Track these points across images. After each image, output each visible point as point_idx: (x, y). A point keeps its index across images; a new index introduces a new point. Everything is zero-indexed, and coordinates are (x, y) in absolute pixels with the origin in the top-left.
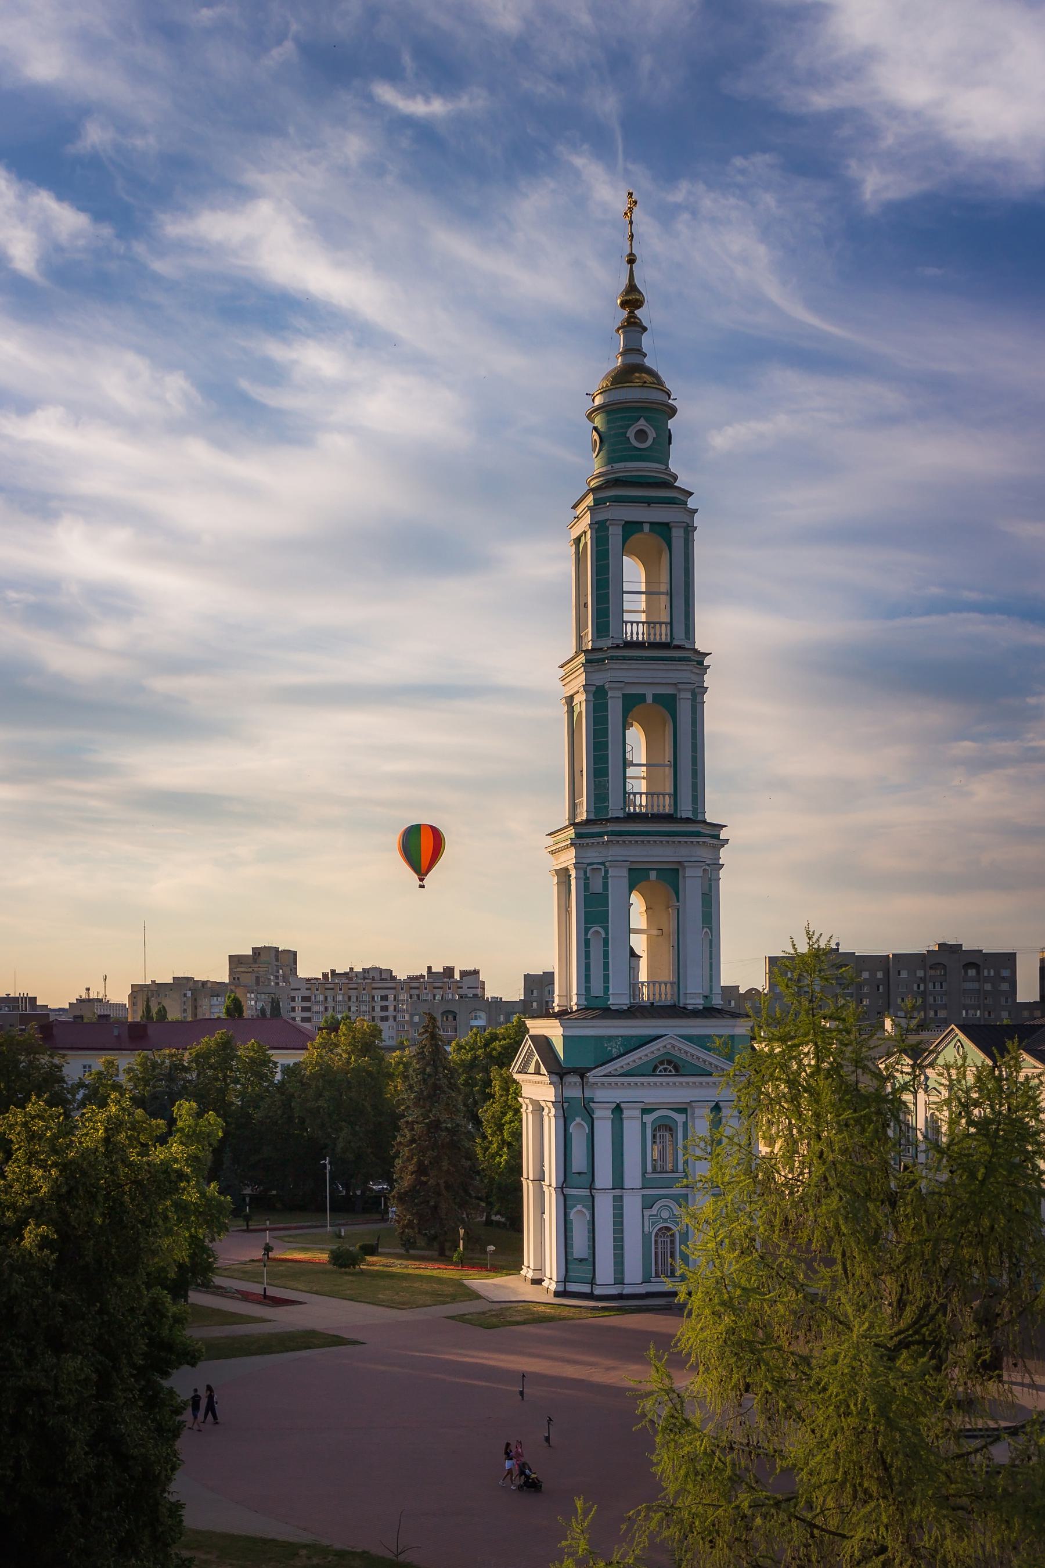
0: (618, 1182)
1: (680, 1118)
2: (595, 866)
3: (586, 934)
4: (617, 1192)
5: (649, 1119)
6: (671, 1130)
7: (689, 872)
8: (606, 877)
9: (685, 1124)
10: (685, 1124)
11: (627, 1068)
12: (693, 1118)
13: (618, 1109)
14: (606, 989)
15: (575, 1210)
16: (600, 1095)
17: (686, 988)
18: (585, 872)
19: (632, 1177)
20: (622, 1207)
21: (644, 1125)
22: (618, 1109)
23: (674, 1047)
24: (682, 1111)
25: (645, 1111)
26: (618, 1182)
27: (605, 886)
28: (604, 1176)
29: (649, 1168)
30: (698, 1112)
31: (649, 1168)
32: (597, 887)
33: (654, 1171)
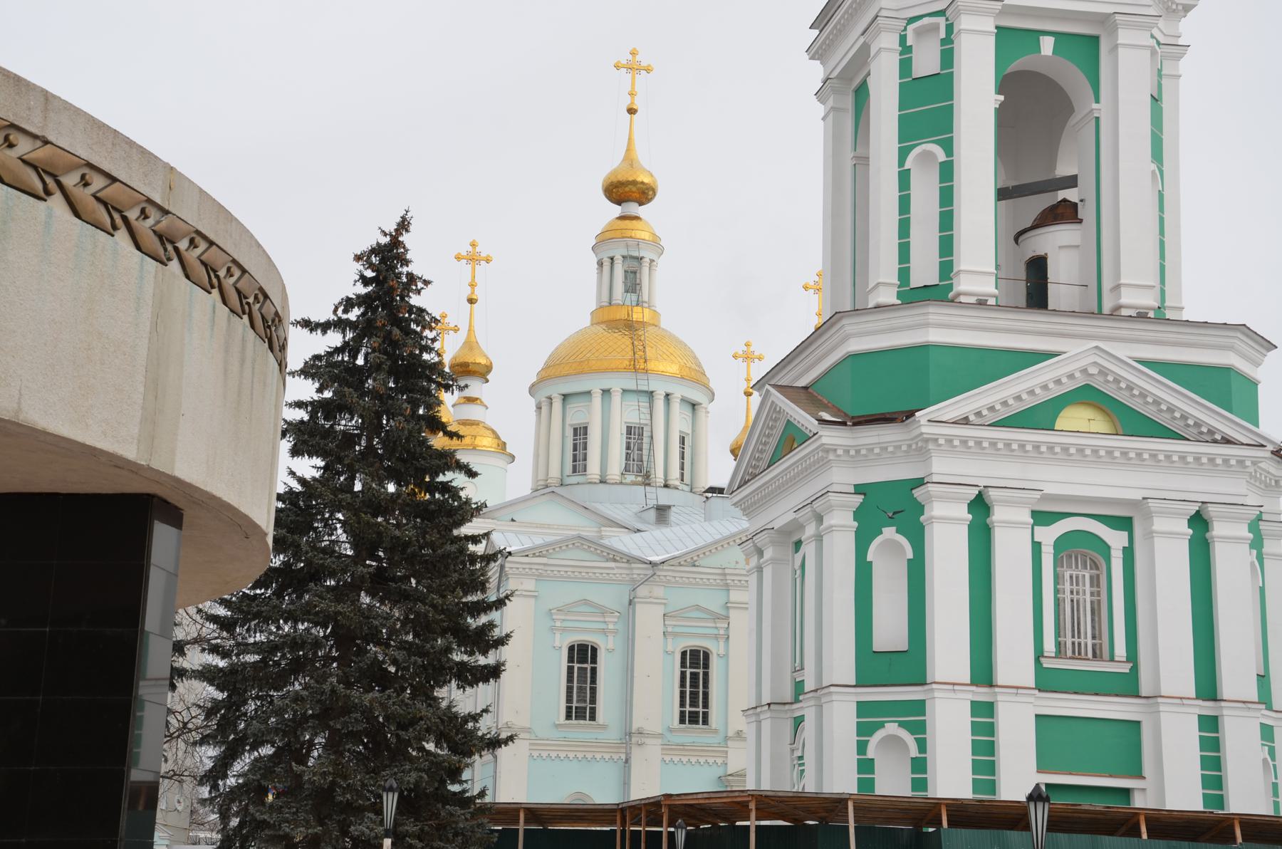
0: (983, 672)
1: (1116, 540)
2: (926, 21)
3: (902, 161)
4: (982, 694)
5: (1048, 535)
6: (1095, 566)
7: (1124, 36)
8: (948, 41)
9: (1129, 553)
10: (1129, 553)
11: (1003, 413)
12: (1150, 535)
13: (980, 505)
14: (947, 269)
15: (880, 734)
16: (941, 466)
17: (1117, 274)
18: (903, 39)
19: (1014, 660)
20: (990, 729)
21: (1037, 547)
22: (980, 505)
23: (1103, 372)
24: (1124, 523)
25: (1042, 518)
26: (983, 672)
27: (948, 57)
28: (949, 653)
29: (1049, 646)
30: (1159, 524)
31: (1049, 646)
32: (926, 62)
33: (1060, 651)
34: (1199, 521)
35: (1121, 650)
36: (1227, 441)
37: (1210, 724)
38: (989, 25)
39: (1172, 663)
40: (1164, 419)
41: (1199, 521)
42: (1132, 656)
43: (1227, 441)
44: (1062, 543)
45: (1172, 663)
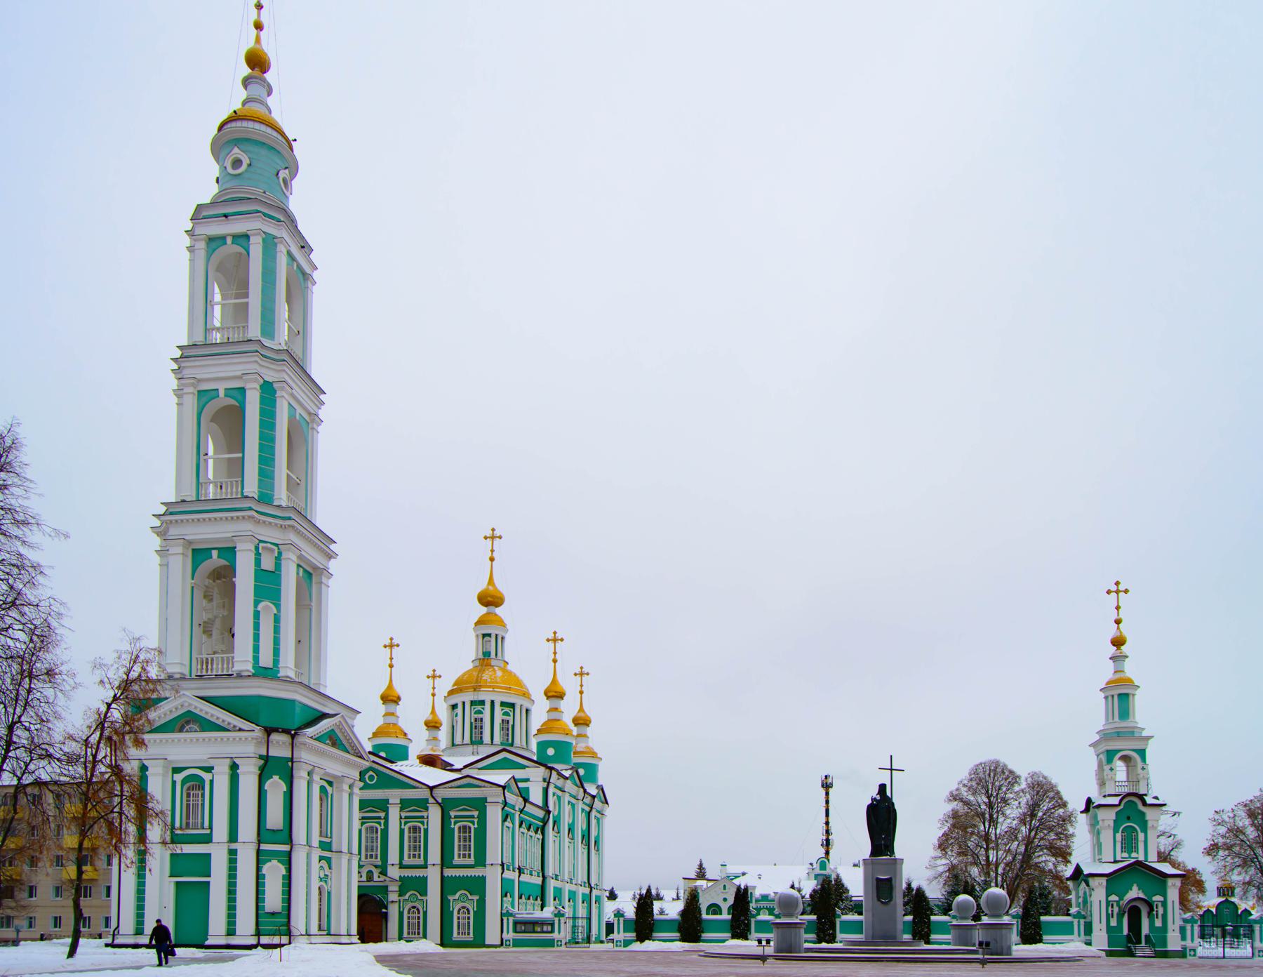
1: (207, 777)
5: (179, 777)
10: (212, 782)
21: (174, 783)
24: (209, 769)
25: (176, 770)
34: (234, 767)
35: (207, 824)
36: (240, 730)
37: (233, 853)
38: (180, 550)
39: (221, 831)
40: (219, 722)
41: (234, 767)
42: (211, 828)
43: (240, 730)
44: (184, 782)
45: (221, 831)
